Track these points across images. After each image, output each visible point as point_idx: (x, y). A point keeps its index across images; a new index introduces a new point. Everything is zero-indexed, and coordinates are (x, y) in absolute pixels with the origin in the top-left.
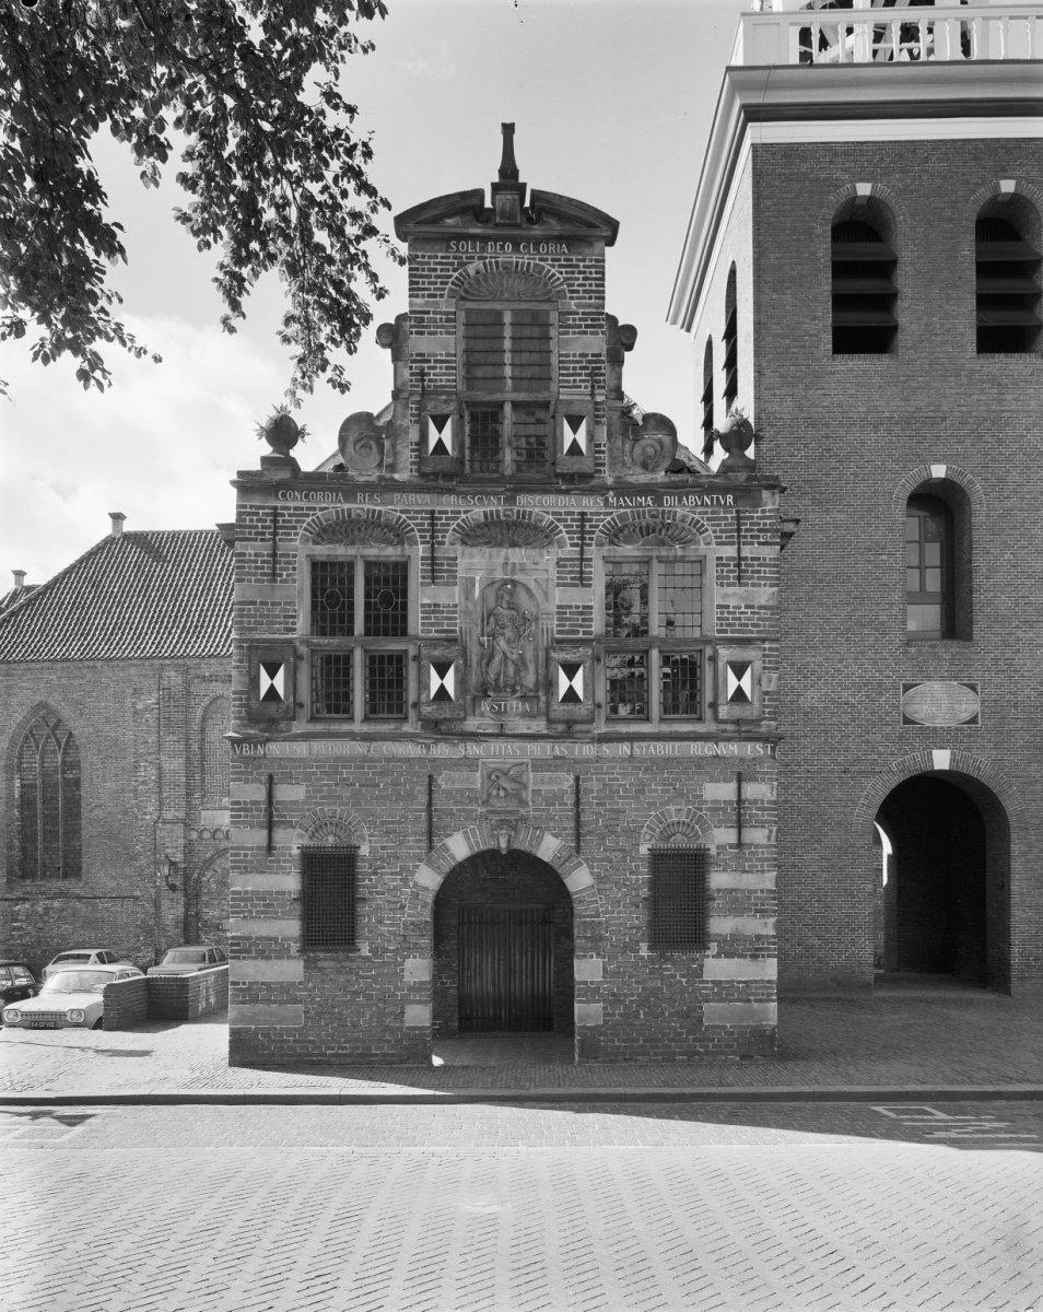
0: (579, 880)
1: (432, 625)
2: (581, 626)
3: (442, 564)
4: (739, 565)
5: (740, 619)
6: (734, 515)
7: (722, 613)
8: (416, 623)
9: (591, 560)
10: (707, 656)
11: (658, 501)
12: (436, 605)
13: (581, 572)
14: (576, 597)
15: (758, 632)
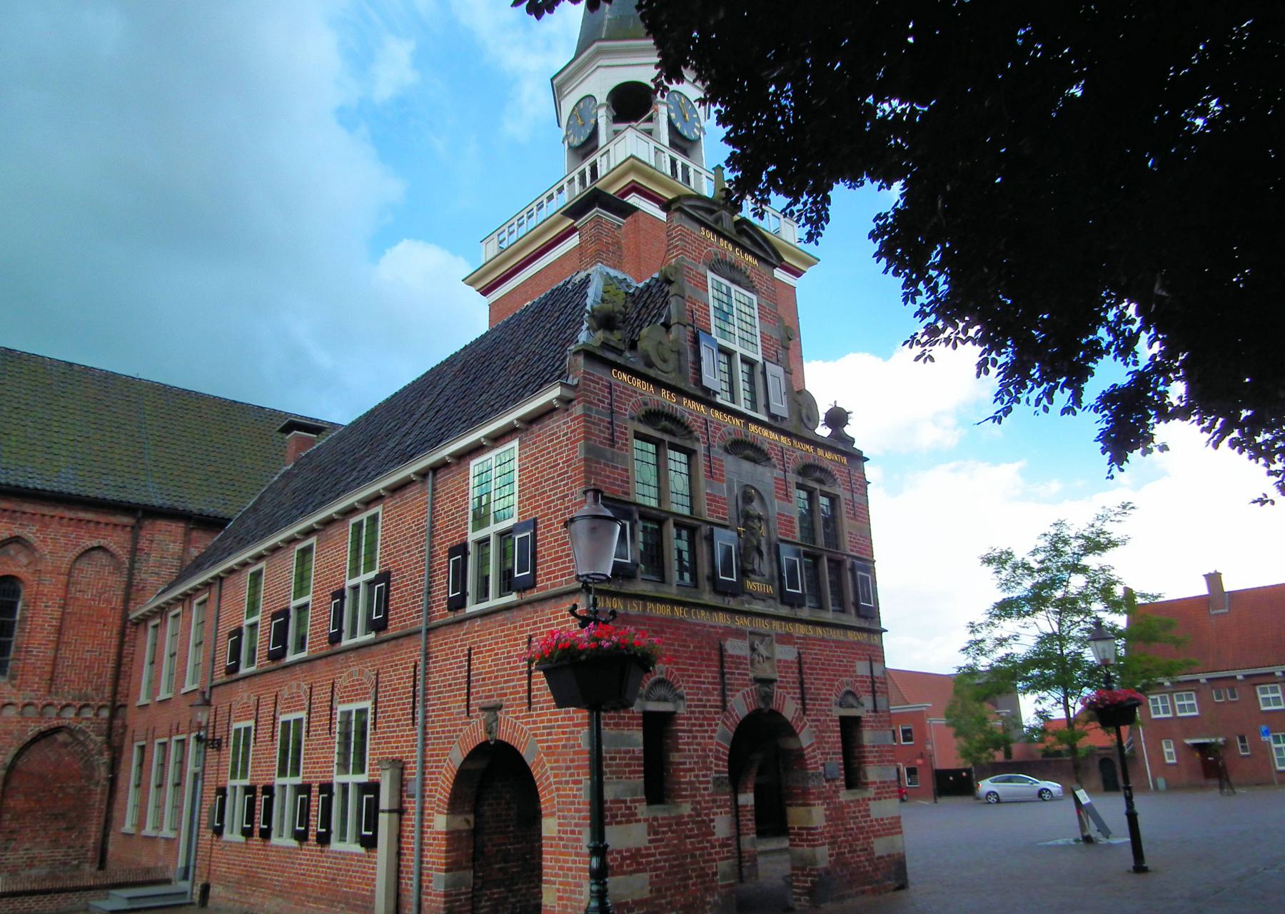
0: (805, 739)
1: (714, 511)
11: (815, 450)
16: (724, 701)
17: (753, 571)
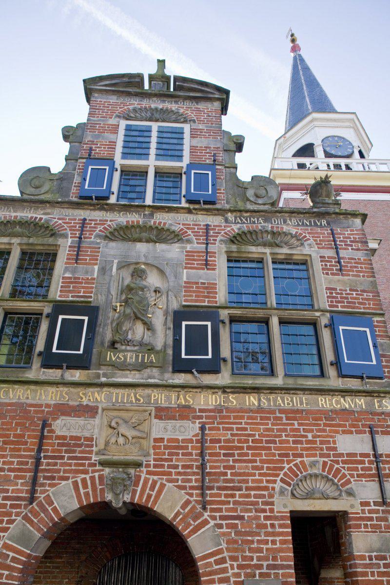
2: (208, 297)
3: (88, 251)
4: (339, 262)
5: (347, 298)
6: (329, 231)
7: (331, 293)
8: (56, 292)
9: (215, 253)
10: (323, 324)
12: (75, 278)
13: (206, 260)
14: (203, 276)
15: (364, 308)
16: (33, 491)
17: (128, 342)
